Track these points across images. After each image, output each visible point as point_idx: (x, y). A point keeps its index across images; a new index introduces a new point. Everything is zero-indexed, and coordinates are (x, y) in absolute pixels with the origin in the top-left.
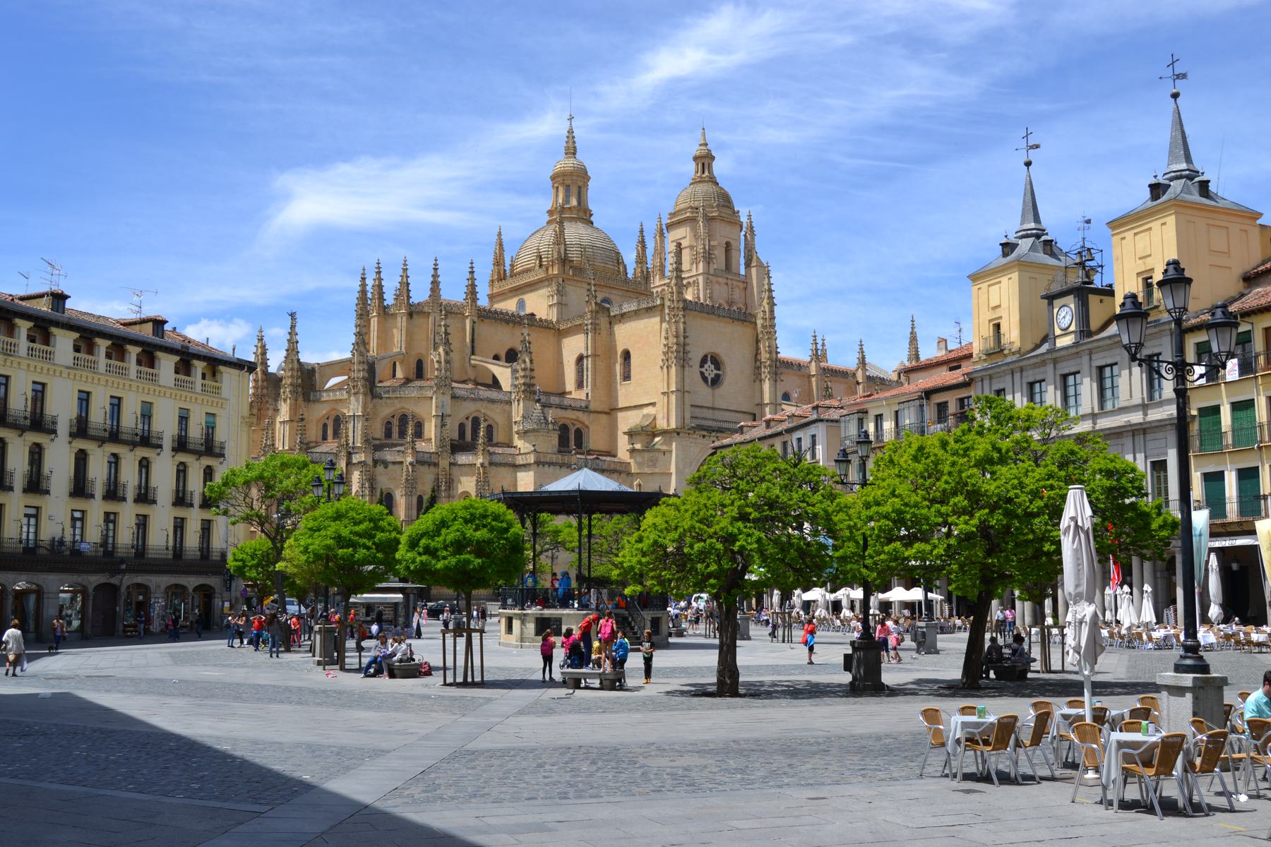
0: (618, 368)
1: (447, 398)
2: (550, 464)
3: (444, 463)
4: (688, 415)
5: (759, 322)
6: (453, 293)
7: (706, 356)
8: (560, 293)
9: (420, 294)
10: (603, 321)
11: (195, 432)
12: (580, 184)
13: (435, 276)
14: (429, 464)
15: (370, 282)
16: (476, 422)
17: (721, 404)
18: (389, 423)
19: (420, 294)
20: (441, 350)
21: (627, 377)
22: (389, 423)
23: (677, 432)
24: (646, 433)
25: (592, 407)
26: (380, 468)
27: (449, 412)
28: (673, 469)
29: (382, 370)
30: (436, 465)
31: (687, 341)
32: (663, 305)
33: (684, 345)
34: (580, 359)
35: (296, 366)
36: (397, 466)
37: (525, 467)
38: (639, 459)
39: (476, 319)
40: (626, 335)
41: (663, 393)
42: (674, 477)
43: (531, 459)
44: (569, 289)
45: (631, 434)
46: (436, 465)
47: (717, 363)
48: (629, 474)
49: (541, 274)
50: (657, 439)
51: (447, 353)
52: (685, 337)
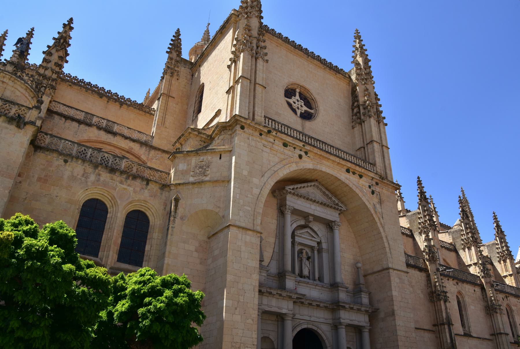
21: (199, 111)
25: (155, 143)
38: (182, 166)
47: (307, 101)
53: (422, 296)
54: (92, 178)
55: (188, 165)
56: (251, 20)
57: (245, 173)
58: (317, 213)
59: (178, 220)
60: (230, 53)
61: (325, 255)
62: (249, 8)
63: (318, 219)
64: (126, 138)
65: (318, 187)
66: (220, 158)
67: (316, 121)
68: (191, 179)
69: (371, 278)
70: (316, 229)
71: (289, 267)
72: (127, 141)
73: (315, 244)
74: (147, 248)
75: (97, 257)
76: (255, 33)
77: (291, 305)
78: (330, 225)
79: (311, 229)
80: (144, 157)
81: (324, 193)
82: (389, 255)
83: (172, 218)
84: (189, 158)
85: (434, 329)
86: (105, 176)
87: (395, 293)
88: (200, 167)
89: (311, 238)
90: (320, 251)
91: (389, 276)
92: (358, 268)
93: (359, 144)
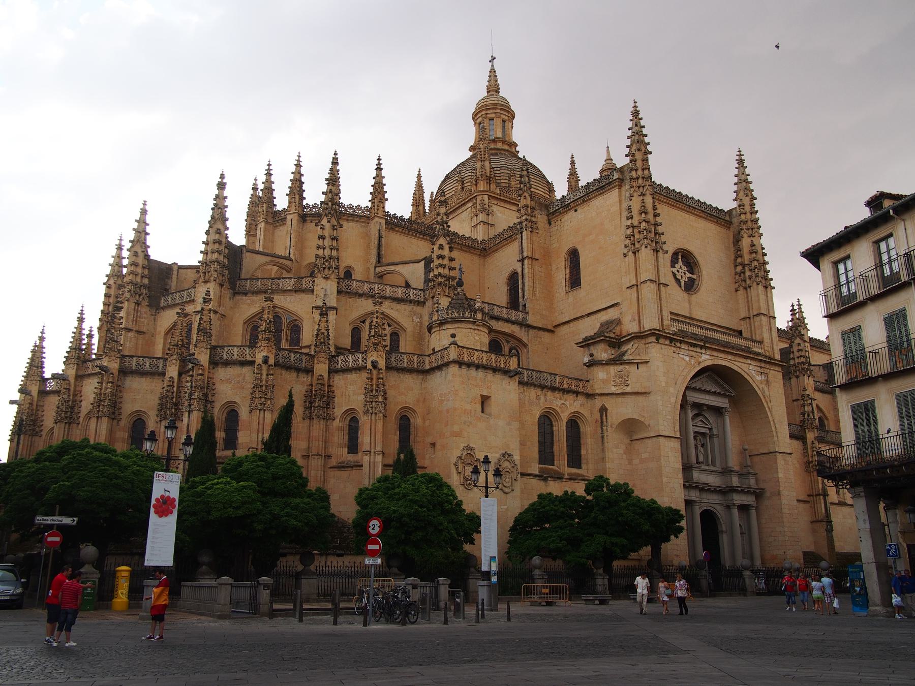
0: (561, 275)
2: (478, 367)
3: (321, 368)
4: (666, 315)
6: (356, 194)
7: (675, 254)
9: (314, 195)
14: (298, 370)
15: (261, 186)
17: (699, 314)
18: (256, 328)
19: (314, 195)
21: (575, 281)
23: (658, 335)
26: (222, 373)
27: (332, 301)
29: (250, 263)
30: (309, 371)
31: (659, 219)
33: (656, 225)
35: (141, 260)
36: (246, 370)
39: (383, 222)
44: (495, 208)
46: (309, 371)
51: (334, 228)
52: (656, 215)
53: (797, 466)
56: (645, 198)
57: (663, 384)
58: (711, 403)
59: (609, 429)
60: (623, 237)
61: (715, 440)
62: (640, 181)
64: (508, 321)
67: (701, 291)
68: (613, 389)
69: (756, 459)
71: (694, 460)
72: (509, 325)
73: (707, 431)
74: (583, 452)
77: (698, 494)
78: (718, 411)
80: (525, 340)
82: (775, 438)
83: (605, 428)
84: (607, 367)
85: (808, 499)
86: (550, 395)
87: (781, 475)
88: (621, 377)
90: (711, 436)
91: (776, 459)
92: (745, 450)
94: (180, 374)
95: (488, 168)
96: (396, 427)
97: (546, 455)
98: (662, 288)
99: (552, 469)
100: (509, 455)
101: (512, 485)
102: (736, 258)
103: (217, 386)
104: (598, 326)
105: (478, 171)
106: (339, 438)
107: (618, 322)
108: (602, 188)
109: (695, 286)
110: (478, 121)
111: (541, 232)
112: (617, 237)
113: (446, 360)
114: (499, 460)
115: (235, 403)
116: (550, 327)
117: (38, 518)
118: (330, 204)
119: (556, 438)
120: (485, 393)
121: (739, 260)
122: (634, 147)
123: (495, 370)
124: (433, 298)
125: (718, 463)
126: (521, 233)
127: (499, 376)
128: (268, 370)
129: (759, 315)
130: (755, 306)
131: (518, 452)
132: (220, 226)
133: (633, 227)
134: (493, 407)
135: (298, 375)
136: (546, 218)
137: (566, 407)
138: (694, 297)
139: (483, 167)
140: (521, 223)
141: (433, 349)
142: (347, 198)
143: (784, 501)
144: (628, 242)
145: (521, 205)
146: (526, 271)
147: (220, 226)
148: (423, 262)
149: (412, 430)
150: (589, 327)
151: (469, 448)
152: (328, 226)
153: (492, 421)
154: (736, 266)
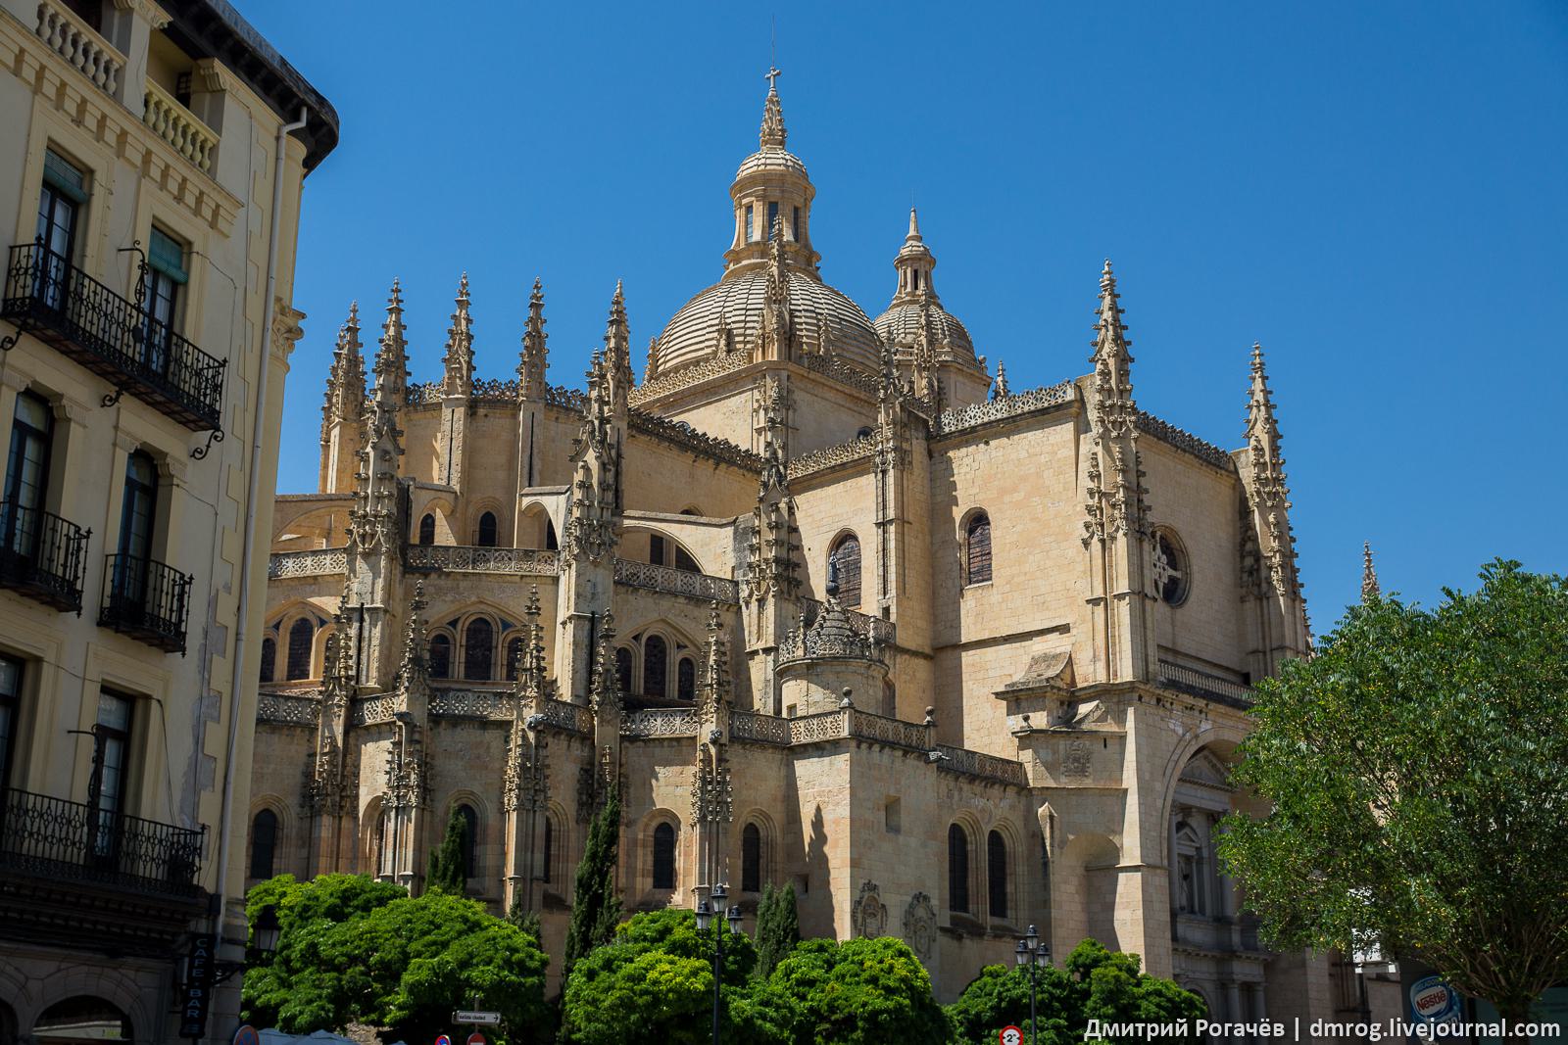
1: (604, 578)
4: (1153, 653)
5: (1247, 474)
8: (784, 401)
9: (500, 362)
10: (918, 447)
11: (110, 262)
12: (799, 202)
13: (535, 321)
16: (656, 647)
17: (1187, 644)
20: (591, 457)
22: (441, 639)
24: (1057, 695)
25: (903, 638)
28: (1130, 779)
30: (587, 738)
32: (1081, 401)
34: (845, 540)
36: (492, 736)
37: (820, 749)
39: (624, 426)
40: (976, 475)
41: (1094, 602)
42: (1132, 802)
43: (844, 727)
44: (799, 396)
45: (1016, 698)
48: (1023, 788)
49: (736, 365)
50: (1084, 709)
54: (956, 793)
55: (1054, 754)
57: (1147, 776)
60: (1081, 508)
61: (1206, 869)
63: (1200, 810)
65: (1206, 758)
66: (1105, 746)
70: (1194, 825)
73: (1192, 852)
74: (1010, 888)
75: (966, 910)
76: (1133, 477)
78: (1213, 817)
79: (1192, 828)
81: (1214, 766)
84: (1054, 741)
86: (966, 787)
88: (1076, 760)
89: (1189, 843)
90: (1200, 861)
93: (1252, 645)
94: (346, 733)
95: (787, 317)
96: (740, 843)
97: (959, 897)
98: (1148, 602)
99: (966, 919)
100: (926, 898)
101: (929, 950)
102: (1242, 545)
103: (438, 762)
104: (1027, 660)
105: (772, 324)
106: (644, 860)
107: (1070, 662)
108: (1044, 411)
109: (1179, 591)
110: (744, 201)
111: (917, 471)
112: (1071, 508)
113: (830, 735)
114: (911, 906)
115: (472, 793)
116: (927, 650)
117: (461, 1014)
118: (596, 422)
119: (971, 865)
120: (892, 793)
121: (1249, 546)
122: (1107, 348)
123: (907, 750)
124: (761, 602)
125: (1208, 911)
126: (884, 472)
127: (912, 761)
128: (537, 738)
129: (1282, 648)
130: (1274, 633)
131: (937, 891)
132: (389, 447)
133: (1102, 495)
134: (905, 820)
135: (569, 746)
136: (924, 444)
137: (994, 810)
138: (1179, 611)
139: (780, 315)
140: (882, 452)
141: (792, 708)
142: (552, 378)
143: (1312, 978)
144: (1089, 518)
145: (882, 418)
146: (892, 545)
147: (389, 447)
148: (730, 530)
149: (763, 850)
150: (1012, 666)
151: (871, 887)
152: (594, 465)
153: (901, 838)
154: (1242, 557)
